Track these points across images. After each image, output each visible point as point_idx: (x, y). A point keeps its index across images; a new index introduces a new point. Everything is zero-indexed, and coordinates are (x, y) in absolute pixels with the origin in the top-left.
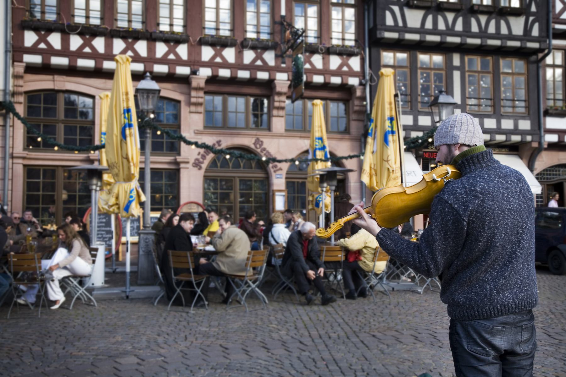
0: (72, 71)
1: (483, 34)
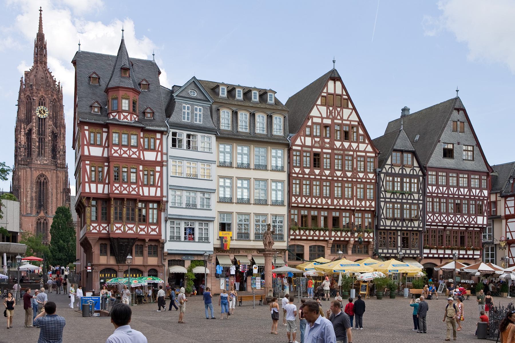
0: (300, 240)
1: (407, 227)
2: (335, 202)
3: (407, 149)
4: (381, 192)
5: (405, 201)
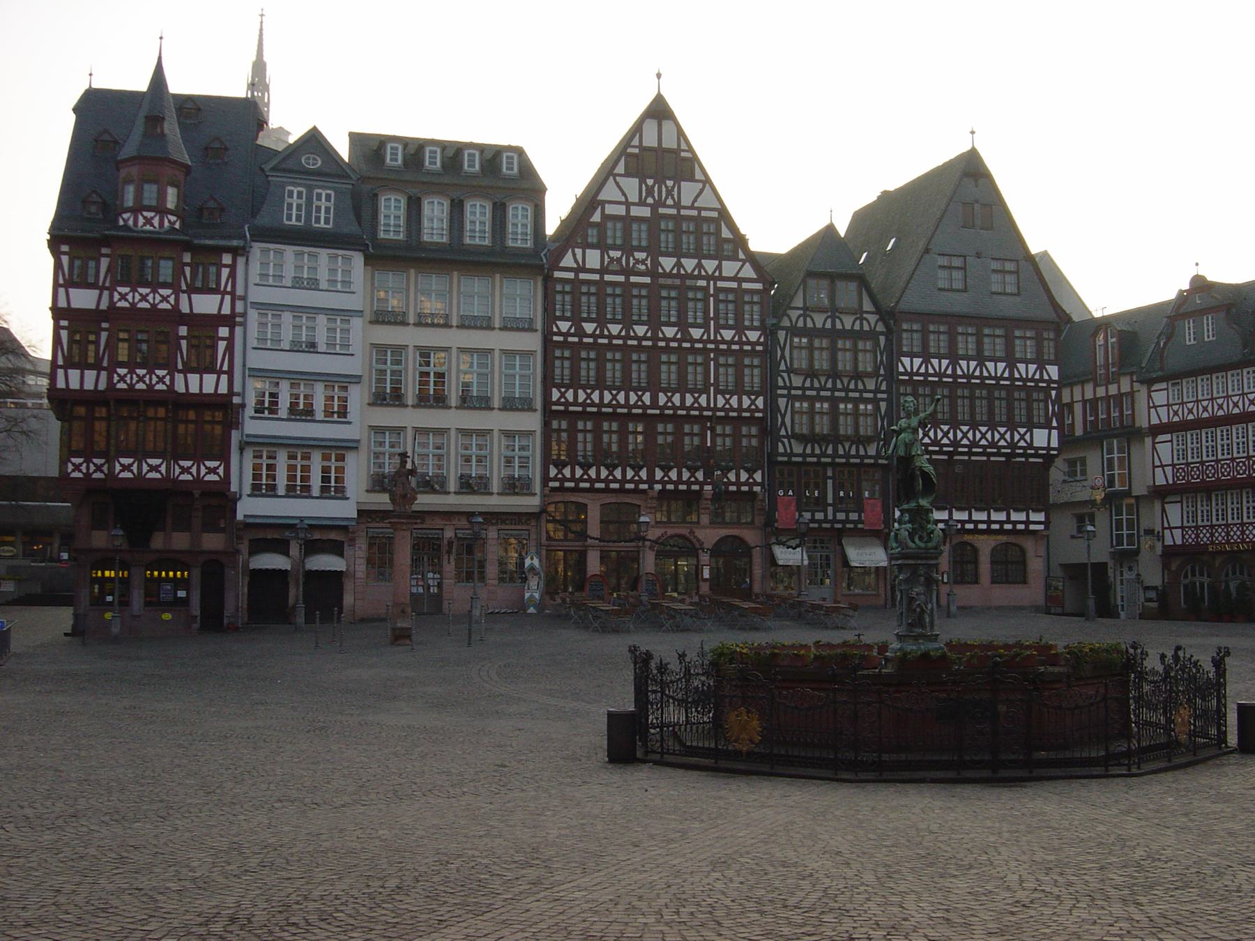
0: (576, 490)
1: (847, 455)
2: (662, 399)
3: (843, 271)
4: (778, 373)
5: (843, 394)
